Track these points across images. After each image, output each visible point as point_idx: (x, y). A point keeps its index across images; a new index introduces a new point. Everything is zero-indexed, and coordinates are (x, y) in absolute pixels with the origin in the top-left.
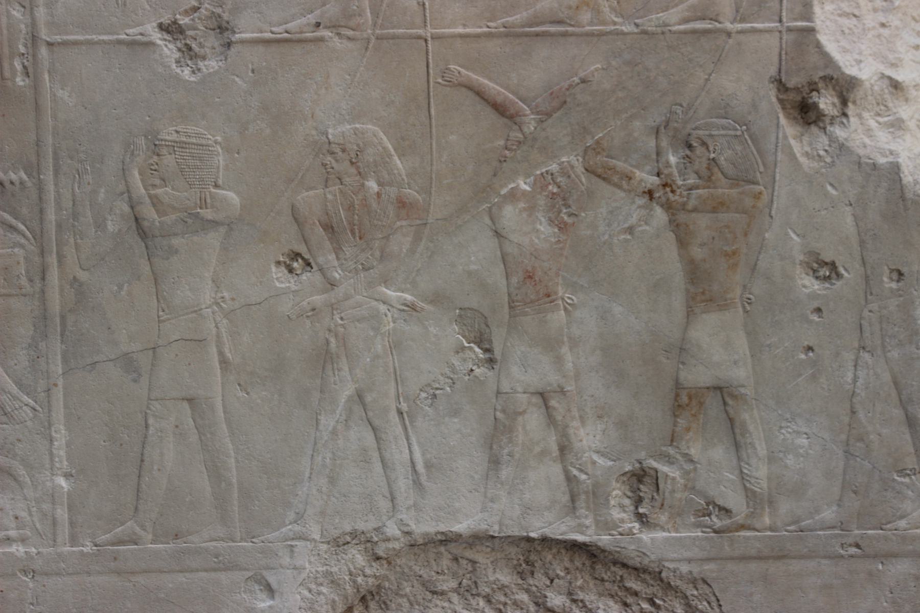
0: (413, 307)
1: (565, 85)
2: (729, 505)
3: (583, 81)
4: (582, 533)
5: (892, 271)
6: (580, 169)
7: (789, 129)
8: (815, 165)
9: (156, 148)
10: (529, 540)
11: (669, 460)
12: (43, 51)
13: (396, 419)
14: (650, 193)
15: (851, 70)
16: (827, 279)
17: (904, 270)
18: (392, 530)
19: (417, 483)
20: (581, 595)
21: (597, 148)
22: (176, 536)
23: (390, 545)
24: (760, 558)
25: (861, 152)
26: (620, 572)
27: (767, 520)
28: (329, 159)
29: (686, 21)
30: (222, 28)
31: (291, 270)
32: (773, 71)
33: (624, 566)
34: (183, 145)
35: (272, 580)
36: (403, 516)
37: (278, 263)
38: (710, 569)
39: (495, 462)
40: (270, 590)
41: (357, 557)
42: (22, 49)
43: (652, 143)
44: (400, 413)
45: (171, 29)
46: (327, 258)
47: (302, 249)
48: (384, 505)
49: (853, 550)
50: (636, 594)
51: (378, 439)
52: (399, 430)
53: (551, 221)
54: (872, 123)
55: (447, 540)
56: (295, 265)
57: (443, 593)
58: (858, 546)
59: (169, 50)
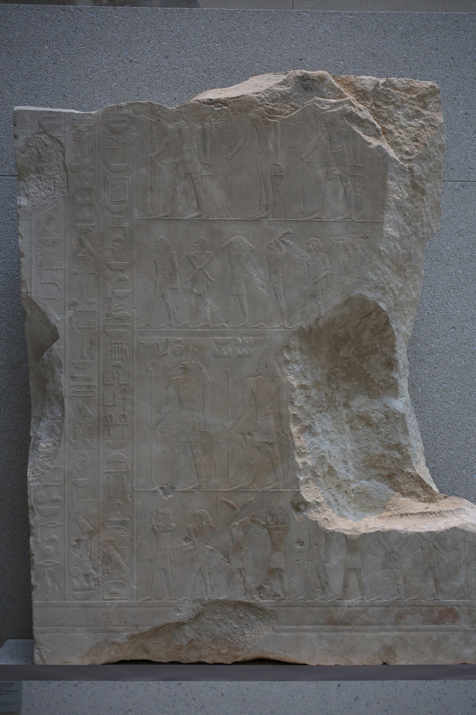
0: (212, 550)
1: (247, 502)
2: (280, 594)
3: (250, 501)
4: (248, 600)
5: (315, 544)
6: (249, 520)
7: (294, 512)
8: (299, 520)
9: (158, 514)
10: (236, 601)
11: (267, 584)
12: (135, 493)
13: (208, 574)
14: (264, 526)
15: (308, 500)
16: (301, 545)
17: (318, 544)
18: (206, 598)
19: (212, 589)
20: (247, 614)
21: (253, 516)
22: (159, 599)
23: (206, 602)
24: (286, 606)
25: (310, 518)
26: (256, 609)
27: (288, 598)
28: (195, 517)
29: (272, 489)
30: (173, 488)
31: (186, 541)
32: (291, 500)
33: (257, 608)
34: (164, 513)
35: (180, 609)
36: (209, 596)
37: (183, 540)
38: (275, 609)
39: (229, 584)
40: (179, 612)
41: (199, 604)
42: (130, 492)
43: (265, 515)
44: (209, 573)
45: (162, 488)
46: (194, 539)
47: (189, 536)
48: (205, 593)
49: (306, 605)
50: (259, 614)
51: (204, 578)
52: (208, 576)
53: (243, 532)
54: (312, 511)
55: (217, 602)
56: (187, 540)
57: (217, 613)
58: (307, 604)
59: (161, 493)
